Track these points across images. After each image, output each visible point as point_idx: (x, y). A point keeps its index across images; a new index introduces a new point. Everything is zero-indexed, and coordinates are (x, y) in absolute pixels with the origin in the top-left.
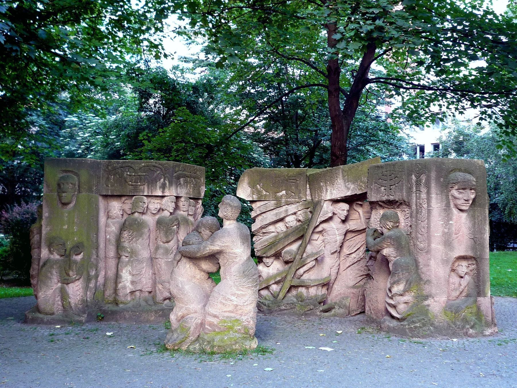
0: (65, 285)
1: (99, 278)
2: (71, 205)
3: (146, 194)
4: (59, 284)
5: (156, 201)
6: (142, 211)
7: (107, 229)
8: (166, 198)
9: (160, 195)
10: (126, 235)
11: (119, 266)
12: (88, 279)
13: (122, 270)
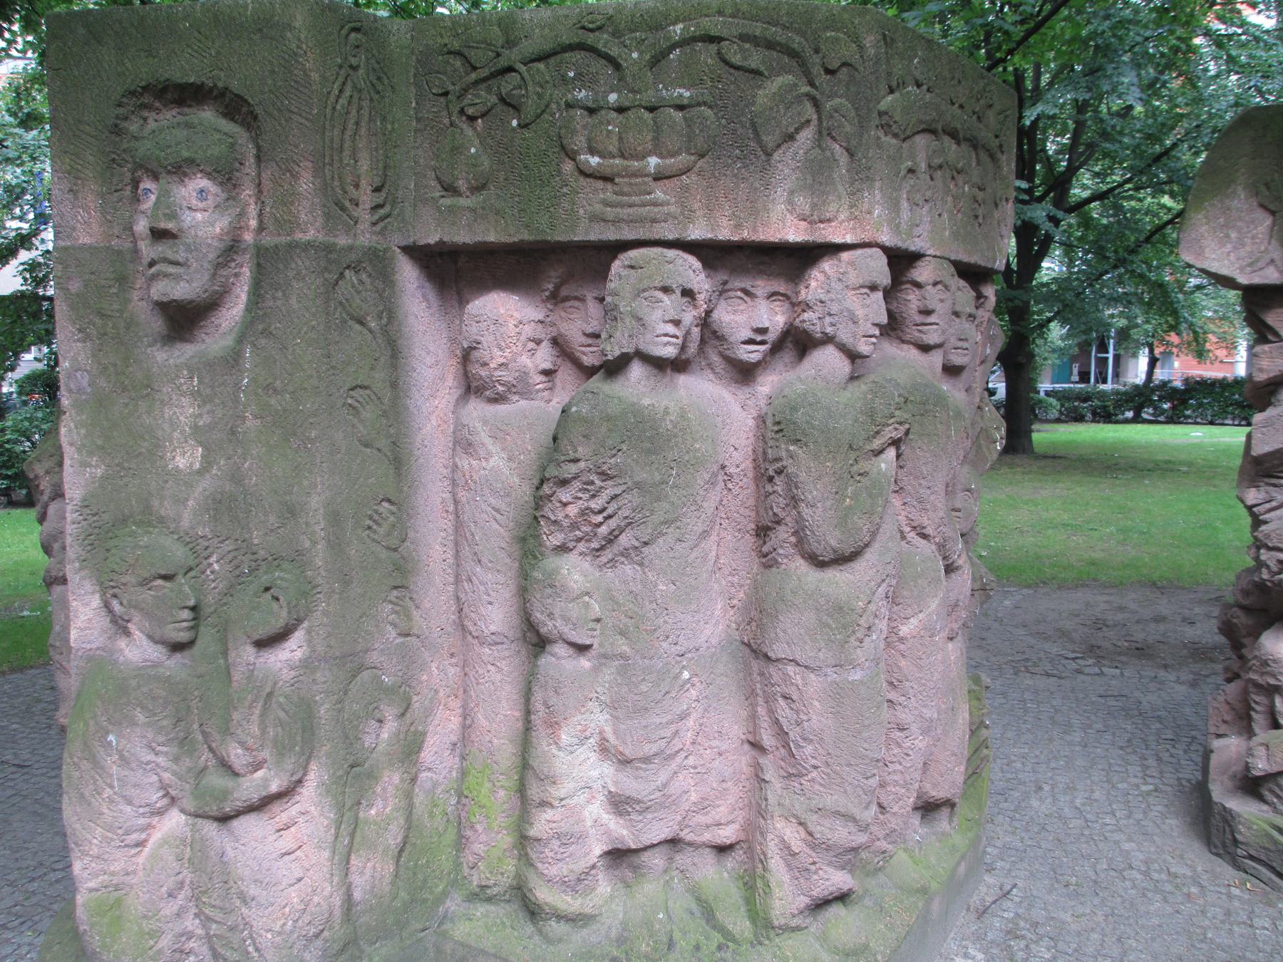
0: (210, 828)
2: (234, 312)
4: (175, 821)
5: (762, 286)
6: (670, 352)
8: (827, 265)
10: (572, 510)
11: (538, 705)
12: (353, 779)
13: (553, 725)
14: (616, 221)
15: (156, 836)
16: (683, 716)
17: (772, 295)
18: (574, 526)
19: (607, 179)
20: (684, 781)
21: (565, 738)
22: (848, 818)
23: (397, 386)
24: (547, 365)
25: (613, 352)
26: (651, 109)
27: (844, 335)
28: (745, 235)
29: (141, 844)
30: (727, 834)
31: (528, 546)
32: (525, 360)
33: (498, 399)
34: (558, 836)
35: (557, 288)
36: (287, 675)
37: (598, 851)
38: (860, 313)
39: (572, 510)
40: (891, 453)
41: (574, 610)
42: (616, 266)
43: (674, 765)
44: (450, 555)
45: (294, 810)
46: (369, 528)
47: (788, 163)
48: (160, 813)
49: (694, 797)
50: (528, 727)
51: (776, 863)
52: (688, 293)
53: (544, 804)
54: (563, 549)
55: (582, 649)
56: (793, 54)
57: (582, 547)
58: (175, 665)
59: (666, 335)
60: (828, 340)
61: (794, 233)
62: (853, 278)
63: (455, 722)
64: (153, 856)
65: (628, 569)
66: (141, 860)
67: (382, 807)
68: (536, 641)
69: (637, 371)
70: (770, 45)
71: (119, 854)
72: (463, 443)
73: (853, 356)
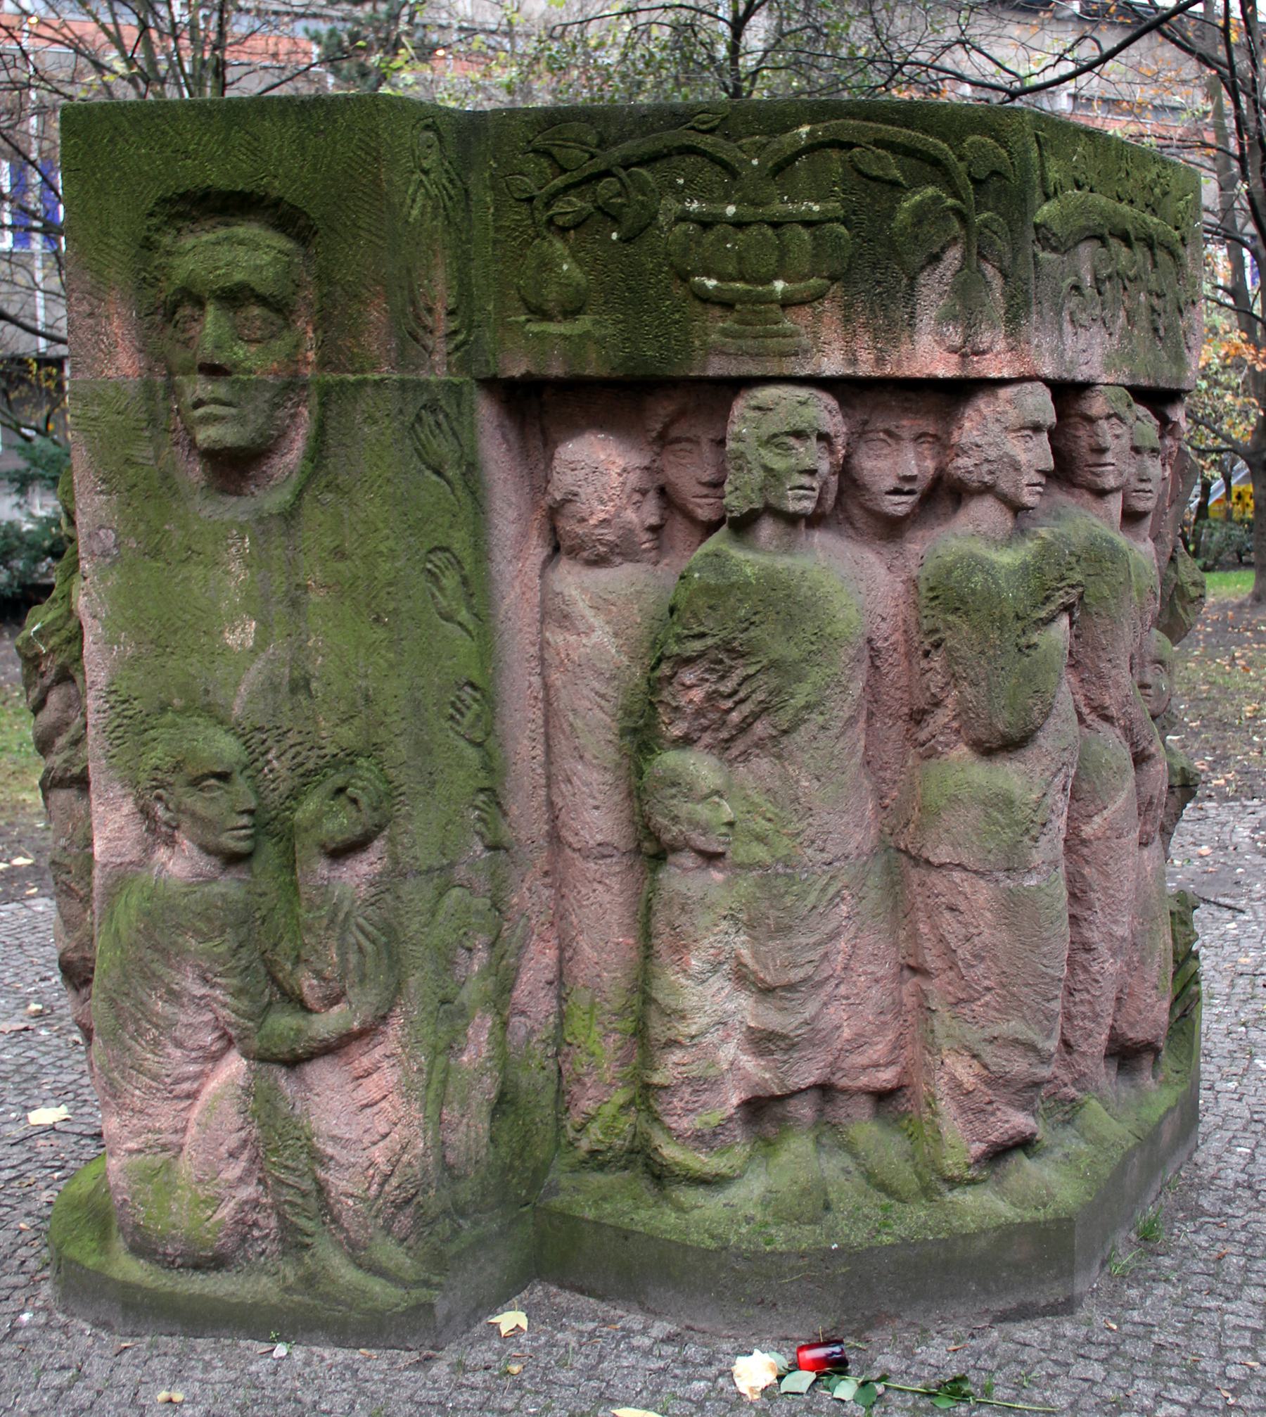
0: (280, 1073)
1: (520, 994)
3: (832, 365)
4: (235, 1066)
5: (908, 426)
6: (808, 506)
7: (557, 637)
8: (984, 404)
9: (942, 371)
13: (680, 948)
14: (741, 354)
15: (213, 1085)
16: (833, 936)
17: (919, 438)
18: (699, 713)
19: (728, 305)
20: (836, 1013)
21: (695, 964)
22: (1031, 1047)
23: (482, 553)
24: (654, 520)
25: (736, 503)
26: (775, 225)
27: (1005, 485)
28: (888, 370)
29: (192, 1096)
30: (886, 1077)
31: (641, 736)
32: (630, 515)
33: (599, 562)
34: (689, 1081)
35: (666, 427)
36: (364, 891)
37: (735, 1101)
38: (1023, 458)
39: (697, 695)
40: (1064, 620)
41: (703, 812)
42: (740, 407)
43: (823, 996)
44: (539, 751)
45: (378, 1053)
46: (452, 717)
47: (933, 291)
48: (215, 1058)
49: (847, 1033)
50: (648, 953)
51: (946, 1107)
52: (823, 437)
53: (672, 1044)
54: (686, 741)
55: (711, 858)
56: (936, 162)
57: (707, 738)
58: (229, 885)
59: (801, 487)
60: (987, 489)
61: (945, 368)
62: (1012, 416)
63: (550, 956)
64: (208, 1109)
65: (763, 764)
66: (195, 1114)
67: (477, 1048)
68: (652, 850)
69: (767, 529)
70: (907, 151)
71: (166, 1107)
72: (553, 613)
73: (1017, 509)
